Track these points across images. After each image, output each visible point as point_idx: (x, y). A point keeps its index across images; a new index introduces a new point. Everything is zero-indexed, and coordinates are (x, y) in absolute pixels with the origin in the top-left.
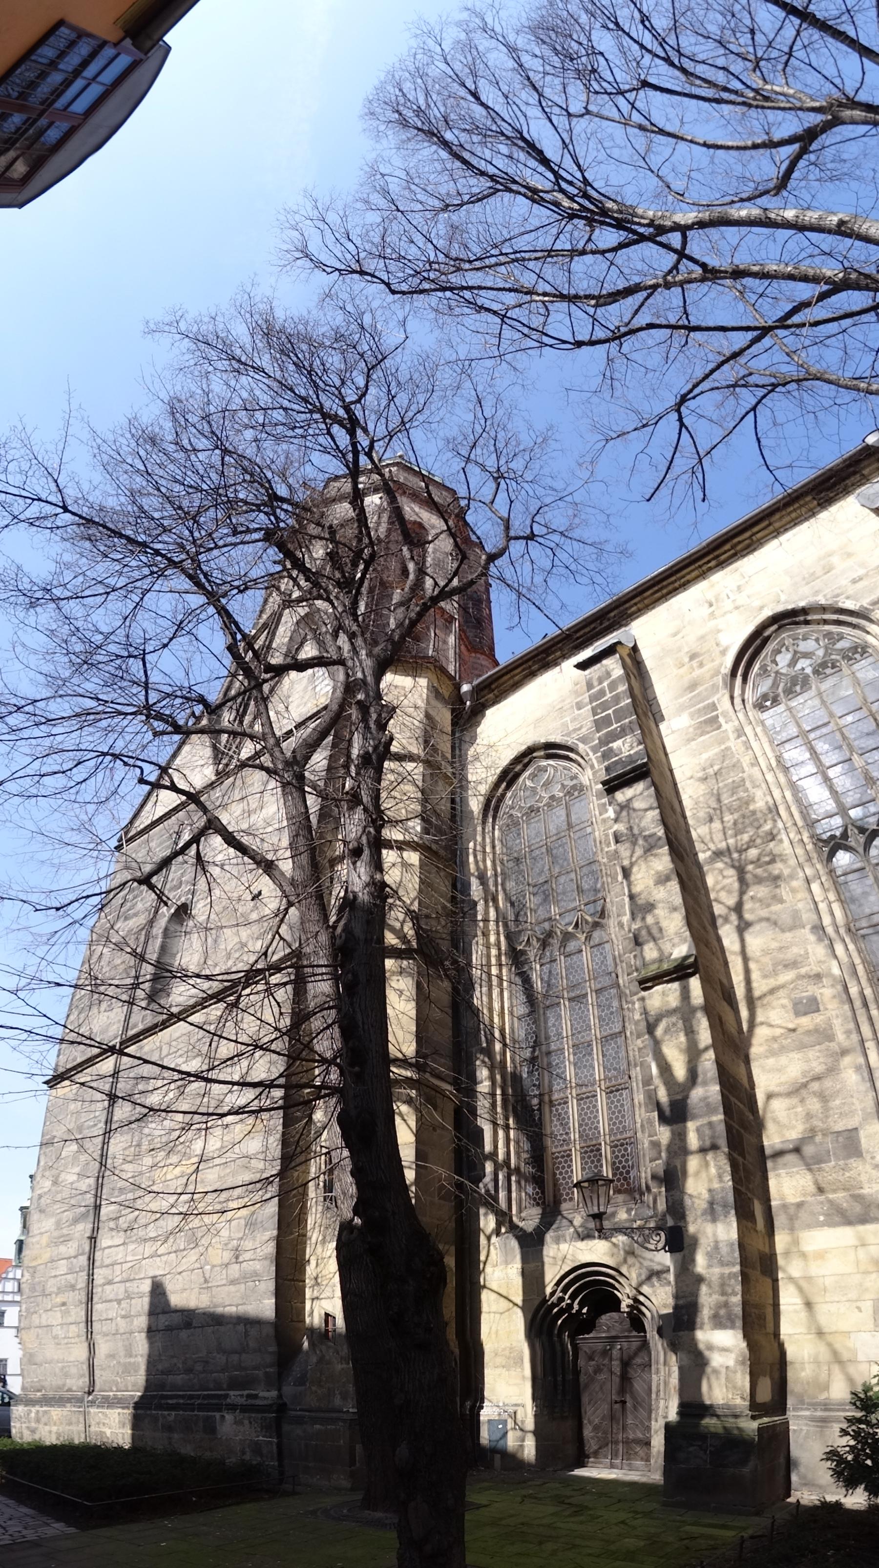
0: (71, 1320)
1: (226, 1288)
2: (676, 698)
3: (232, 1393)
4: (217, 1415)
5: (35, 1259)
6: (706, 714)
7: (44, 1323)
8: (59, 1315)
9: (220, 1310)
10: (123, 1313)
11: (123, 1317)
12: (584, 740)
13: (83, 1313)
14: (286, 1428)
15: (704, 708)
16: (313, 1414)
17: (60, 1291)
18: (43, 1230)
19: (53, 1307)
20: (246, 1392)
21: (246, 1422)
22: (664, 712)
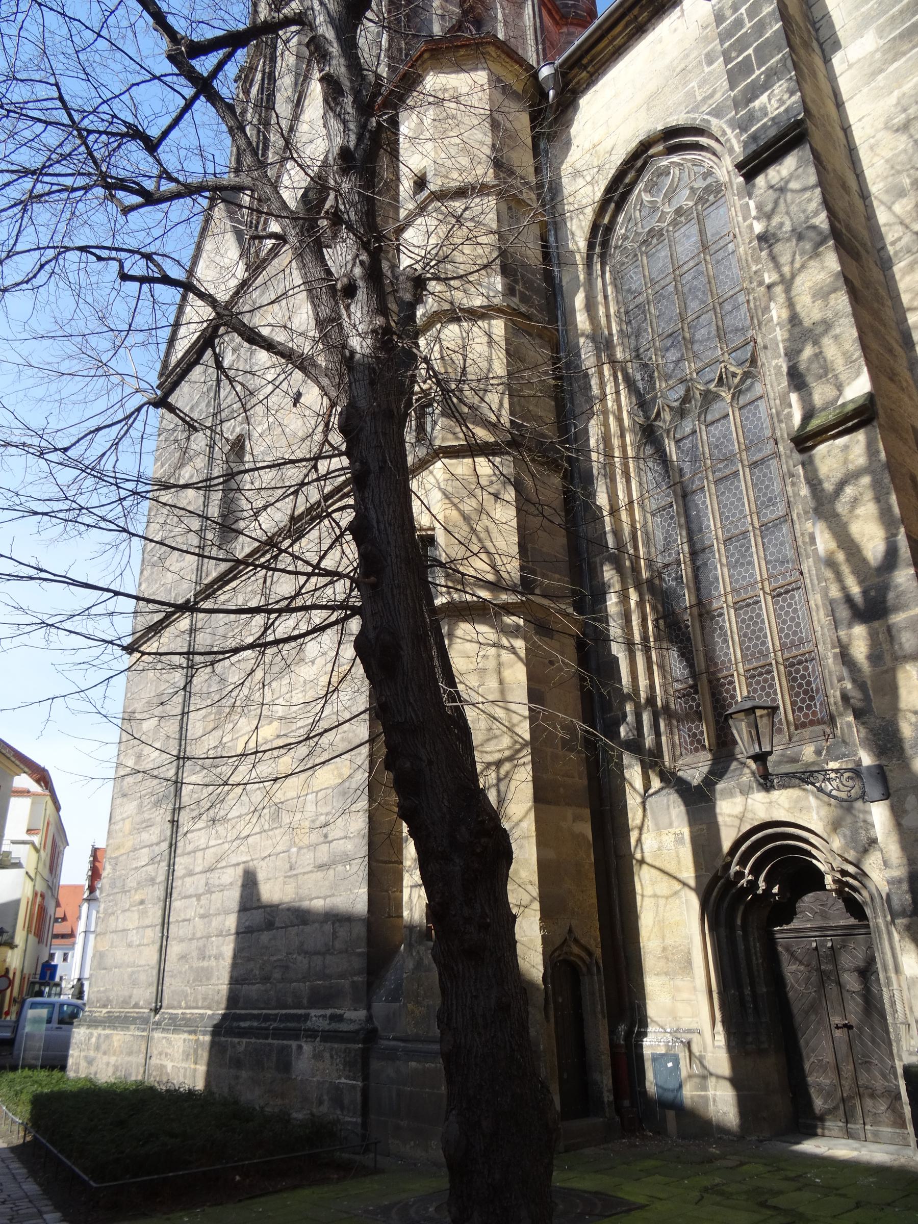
0: (148, 922)
1: (313, 876)
2: (857, 8)
3: (313, 1012)
4: (294, 1044)
5: (118, 848)
6: (903, 22)
7: (120, 927)
8: (136, 915)
9: (306, 904)
10: (202, 911)
11: (202, 917)
12: (717, 112)
13: (159, 913)
14: (375, 1065)
15: (901, 12)
16: (409, 1045)
17: (140, 886)
18: (124, 816)
19: (131, 906)
20: (329, 1012)
21: (327, 1055)
22: (840, 34)
